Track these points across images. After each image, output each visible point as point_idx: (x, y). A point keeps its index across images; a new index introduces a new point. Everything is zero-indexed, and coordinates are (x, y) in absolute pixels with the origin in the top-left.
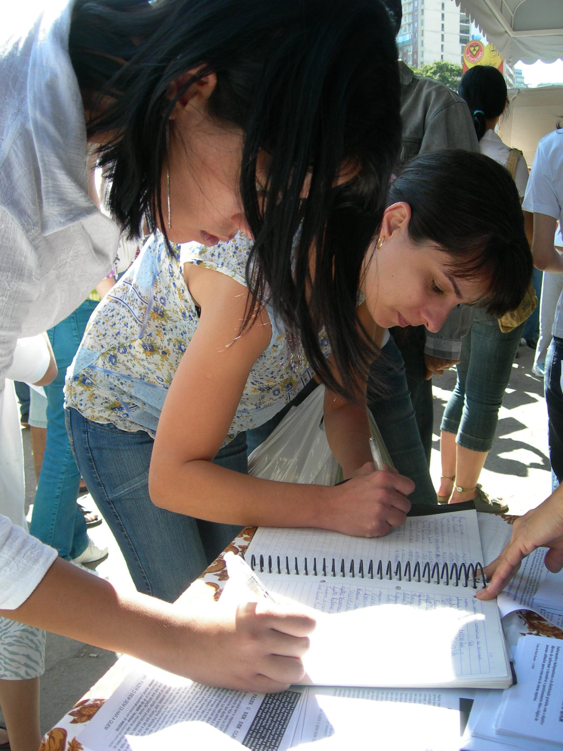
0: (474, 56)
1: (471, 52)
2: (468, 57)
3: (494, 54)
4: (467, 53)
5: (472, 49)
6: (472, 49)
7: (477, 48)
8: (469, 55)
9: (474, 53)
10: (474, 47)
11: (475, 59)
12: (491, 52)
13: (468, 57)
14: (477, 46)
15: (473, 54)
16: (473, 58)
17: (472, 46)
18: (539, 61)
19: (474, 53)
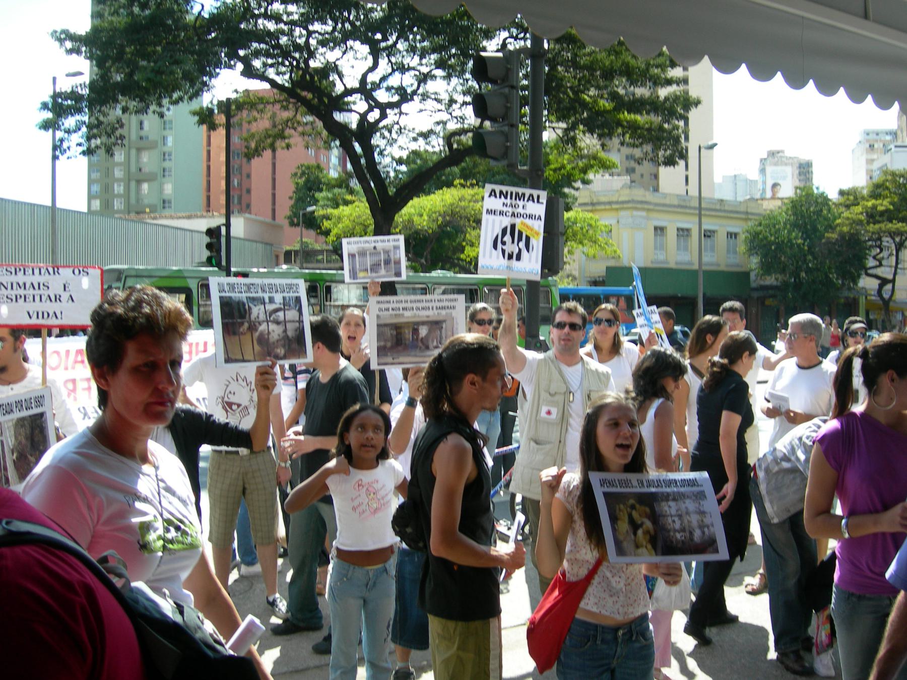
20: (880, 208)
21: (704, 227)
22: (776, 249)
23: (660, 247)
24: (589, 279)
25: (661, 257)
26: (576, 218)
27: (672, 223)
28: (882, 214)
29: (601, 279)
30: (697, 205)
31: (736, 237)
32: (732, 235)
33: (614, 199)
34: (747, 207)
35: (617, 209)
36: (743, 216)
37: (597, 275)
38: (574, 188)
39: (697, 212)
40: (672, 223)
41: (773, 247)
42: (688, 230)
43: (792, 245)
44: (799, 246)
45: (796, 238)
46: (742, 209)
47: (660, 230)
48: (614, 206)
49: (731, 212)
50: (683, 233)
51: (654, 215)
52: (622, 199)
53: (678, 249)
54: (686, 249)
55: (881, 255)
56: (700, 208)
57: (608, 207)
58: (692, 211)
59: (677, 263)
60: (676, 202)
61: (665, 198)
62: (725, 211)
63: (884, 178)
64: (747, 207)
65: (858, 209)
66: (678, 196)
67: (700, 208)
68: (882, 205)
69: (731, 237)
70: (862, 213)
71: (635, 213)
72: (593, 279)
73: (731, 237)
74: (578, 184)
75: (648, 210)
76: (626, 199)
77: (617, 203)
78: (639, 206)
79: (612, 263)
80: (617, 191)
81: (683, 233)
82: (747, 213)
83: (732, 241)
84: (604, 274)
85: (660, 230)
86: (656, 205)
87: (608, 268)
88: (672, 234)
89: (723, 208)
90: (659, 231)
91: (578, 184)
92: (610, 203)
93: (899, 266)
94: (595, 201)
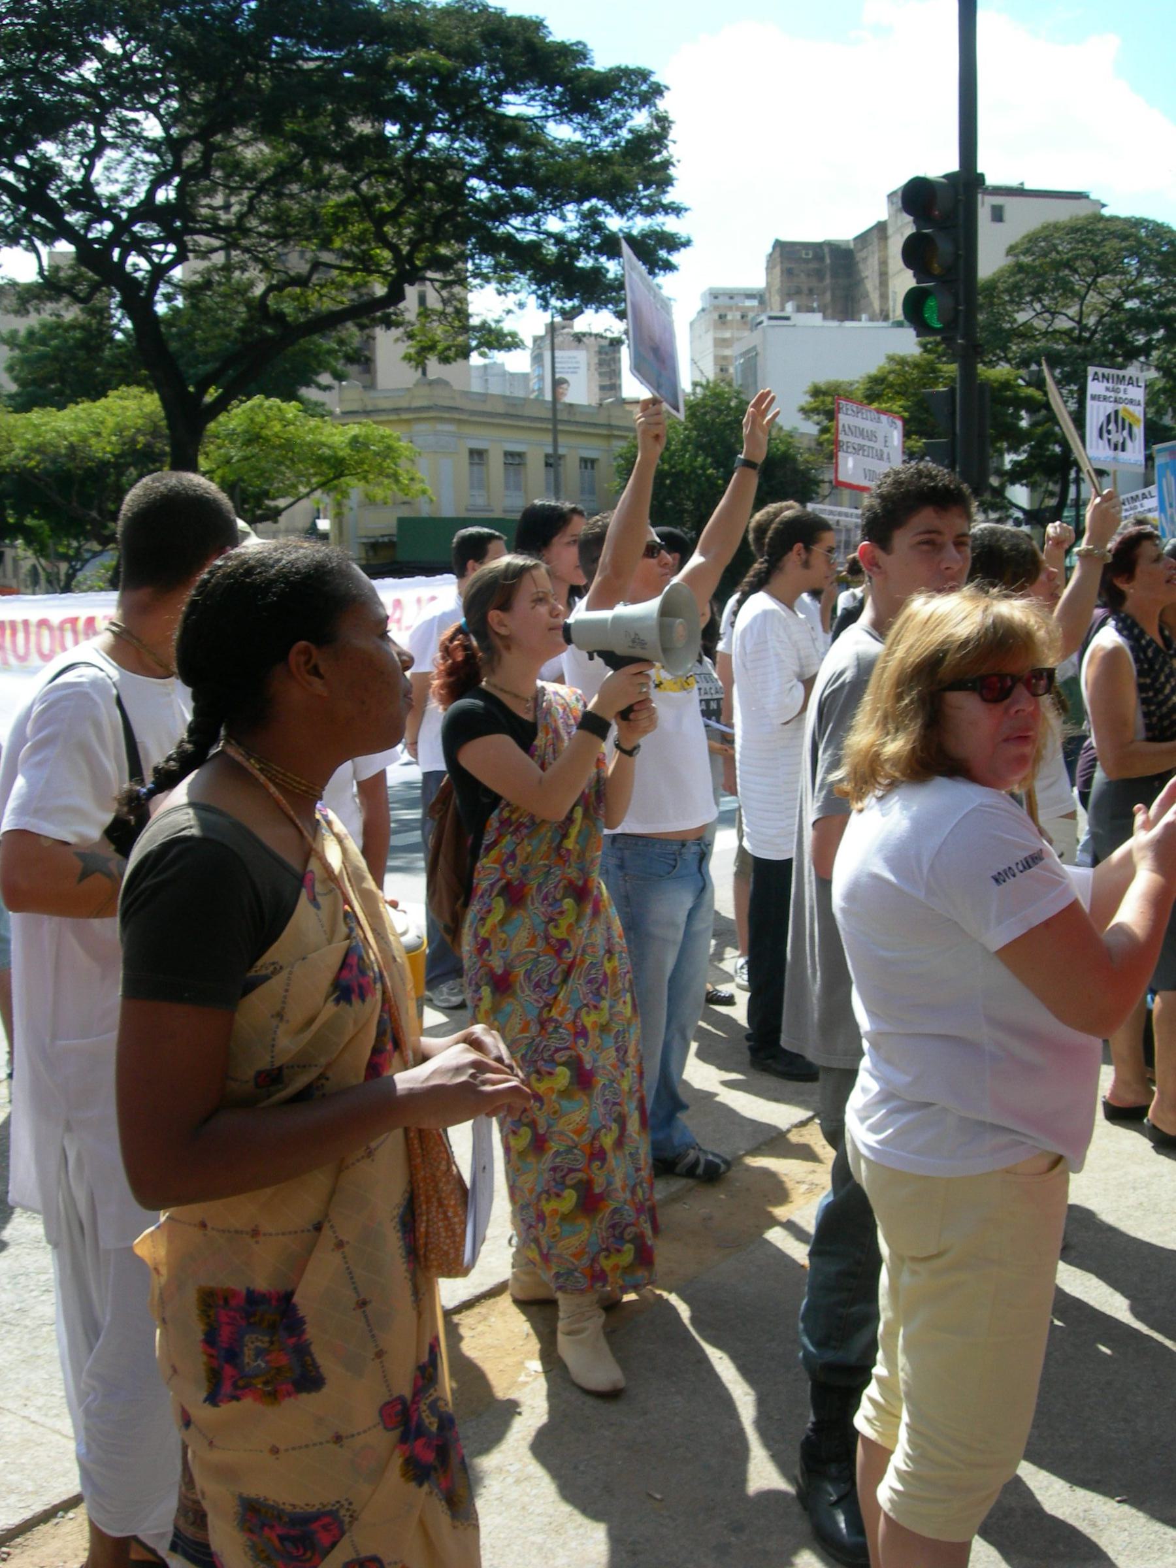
21: (561, 451)
22: (672, 483)
23: (479, 483)
24: (365, 540)
25: (481, 501)
26: (366, 437)
27: (497, 444)
29: (386, 539)
30: (549, 415)
31: (593, 468)
32: (588, 463)
33: (404, 404)
34: (609, 416)
35: (408, 421)
36: (605, 432)
37: (378, 533)
38: (320, 387)
39: (550, 426)
40: (497, 444)
41: (668, 482)
42: (520, 455)
43: (699, 476)
44: (708, 478)
45: (703, 467)
46: (602, 420)
47: (478, 455)
48: (405, 416)
49: (586, 424)
50: (514, 460)
51: (468, 430)
53: (507, 488)
54: (518, 487)
56: (555, 421)
57: (393, 417)
58: (544, 426)
59: (505, 511)
60: (501, 410)
61: (484, 401)
62: (577, 423)
63: (888, 367)
64: (609, 416)
66: (504, 397)
67: (555, 421)
69: (586, 467)
71: (441, 427)
72: (372, 540)
73: (586, 467)
77: (408, 410)
78: (447, 415)
79: (405, 512)
80: (408, 389)
81: (514, 460)
82: (610, 426)
83: (588, 472)
84: (394, 531)
85: (478, 455)
86: (474, 413)
87: (402, 522)
88: (496, 461)
89: (572, 419)
90: (476, 460)
91: (325, 379)
92: (396, 410)
94: (370, 408)
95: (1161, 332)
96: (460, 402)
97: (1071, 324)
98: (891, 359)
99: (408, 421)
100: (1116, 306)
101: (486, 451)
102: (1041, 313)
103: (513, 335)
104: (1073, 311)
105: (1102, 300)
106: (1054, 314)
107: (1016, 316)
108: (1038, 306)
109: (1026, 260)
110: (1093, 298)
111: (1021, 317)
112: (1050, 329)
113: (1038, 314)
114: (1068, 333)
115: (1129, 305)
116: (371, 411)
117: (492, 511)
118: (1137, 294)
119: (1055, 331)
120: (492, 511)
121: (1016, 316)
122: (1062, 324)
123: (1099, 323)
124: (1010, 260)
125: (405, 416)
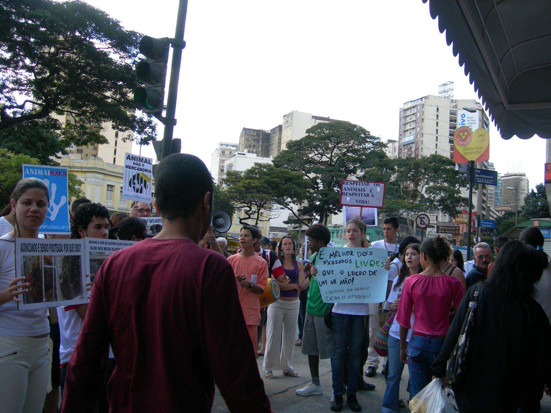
0: (463, 140)
1: (461, 137)
2: (458, 141)
3: (481, 139)
4: (457, 138)
5: (461, 134)
6: (461, 134)
7: (466, 134)
8: (459, 139)
9: (464, 137)
10: (463, 132)
11: (464, 143)
12: (479, 137)
13: (458, 141)
14: (466, 131)
15: (462, 139)
16: (462, 142)
17: (461, 132)
18: (536, 135)
19: (464, 137)
20: (252, 184)
28: (253, 188)
47: (111, 187)
52: (88, 166)
53: (121, 200)
55: (251, 212)
65: (240, 184)
68: (254, 183)
70: (242, 186)
71: (97, 175)
74: (60, 154)
75: (105, 174)
76: (92, 166)
77: (86, 168)
93: (259, 219)
94: (72, 165)
95: (358, 165)
96: (106, 167)
97: (328, 159)
98: (256, 164)
99: (85, 172)
100: (345, 154)
101: (114, 186)
102: (317, 155)
103: (103, 137)
104: (329, 156)
105: (340, 152)
106: (322, 155)
107: (309, 155)
108: (316, 152)
109: (311, 134)
110: (336, 151)
111: (310, 156)
112: (320, 161)
113: (316, 155)
114: (326, 162)
115: (350, 154)
116: (72, 167)
117: (114, 208)
118: (351, 152)
119: (322, 161)
120: (114, 208)
121: (309, 155)
122: (325, 159)
123: (337, 160)
124: (307, 134)
125: (83, 170)
